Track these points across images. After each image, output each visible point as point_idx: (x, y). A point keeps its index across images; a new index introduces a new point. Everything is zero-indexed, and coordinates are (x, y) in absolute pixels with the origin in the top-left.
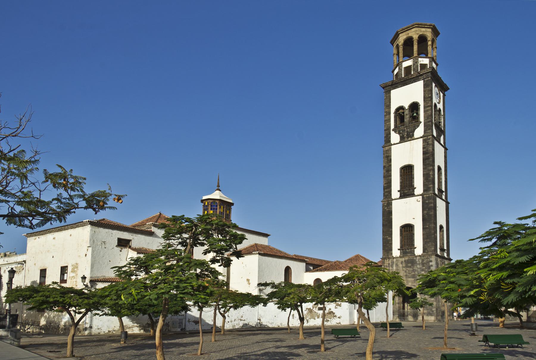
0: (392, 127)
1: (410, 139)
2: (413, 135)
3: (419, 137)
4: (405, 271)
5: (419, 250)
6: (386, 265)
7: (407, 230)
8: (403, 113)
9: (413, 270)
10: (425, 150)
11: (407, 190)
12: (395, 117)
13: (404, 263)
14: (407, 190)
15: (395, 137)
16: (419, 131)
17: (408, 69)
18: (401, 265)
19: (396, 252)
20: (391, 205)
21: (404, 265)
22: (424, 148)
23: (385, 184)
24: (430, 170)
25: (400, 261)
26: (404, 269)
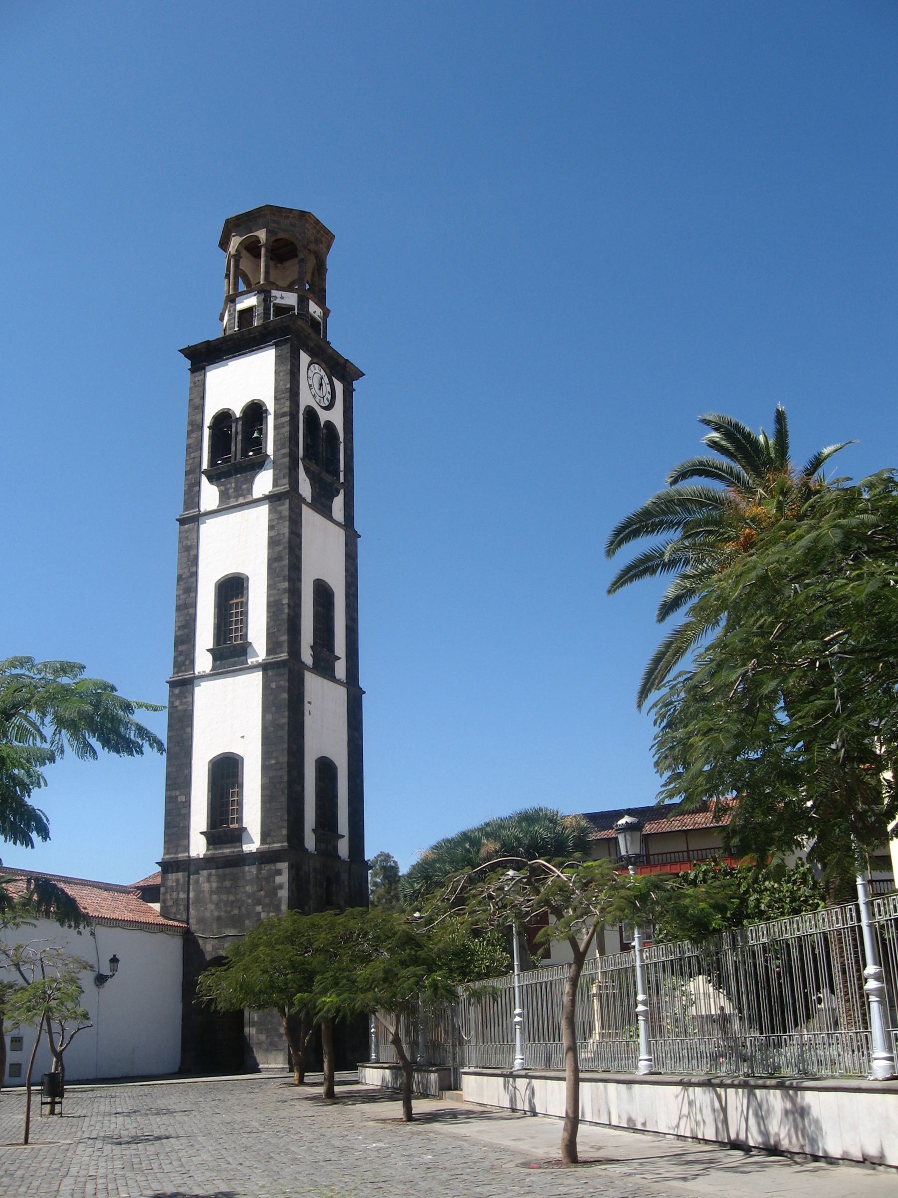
0: (205, 465)
1: (241, 500)
2: (250, 491)
4: (217, 905)
10: (273, 533)
12: (213, 438)
14: (230, 653)
15: (210, 495)
16: (264, 483)
17: (247, 314)
18: (206, 886)
21: (214, 885)
22: (271, 528)
26: (215, 897)
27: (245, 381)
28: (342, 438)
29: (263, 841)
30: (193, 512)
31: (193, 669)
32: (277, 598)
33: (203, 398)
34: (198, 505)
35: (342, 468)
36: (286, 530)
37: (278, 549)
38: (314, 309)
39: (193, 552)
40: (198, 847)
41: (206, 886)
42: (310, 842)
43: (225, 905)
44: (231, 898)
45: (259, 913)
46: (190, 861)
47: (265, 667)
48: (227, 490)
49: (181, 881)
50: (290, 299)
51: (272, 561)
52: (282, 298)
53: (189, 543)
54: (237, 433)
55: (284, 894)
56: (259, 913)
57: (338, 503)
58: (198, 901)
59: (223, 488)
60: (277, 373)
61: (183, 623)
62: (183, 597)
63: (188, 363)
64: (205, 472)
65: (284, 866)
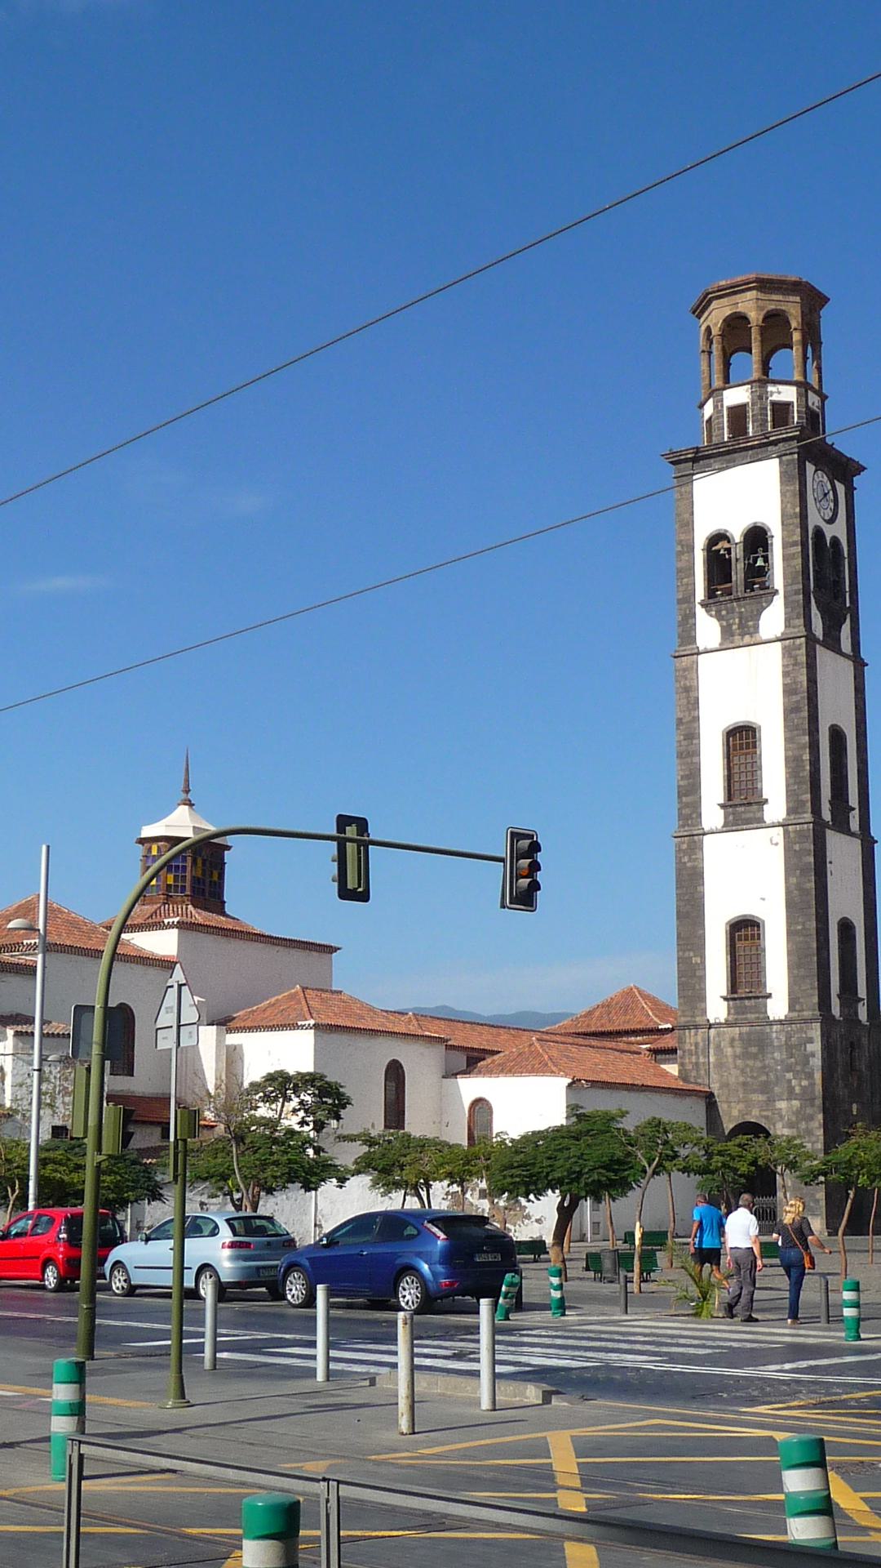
0: (700, 593)
1: (747, 639)
2: (756, 628)
3: (772, 637)
4: (743, 1071)
5: (778, 1007)
7: (744, 930)
8: (729, 550)
9: (764, 1067)
10: (788, 681)
11: (743, 804)
13: (737, 1043)
15: (707, 629)
16: (773, 619)
17: (738, 414)
18: (729, 1051)
19: (717, 1009)
21: (738, 1050)
22: (785, 674)
23: (682, 778)
26: (739, 1062)
27: (743, 497)
29: (791, 1008)
30: (689, 649)
32: (796, 753)
34: (693, 640)
36: (803, 678)
37: (795, 698)
38: (814, 400)
41: (729, 1051)
42: (836, 1010)
45: (789, 1081)
48: (730, 626)
51: (789, 711)
55: (817, 1062)
56: (789, 1081)
57: (846, 629)
58: (720, 1065)
60: (783, 494)
65: (816, 1031)
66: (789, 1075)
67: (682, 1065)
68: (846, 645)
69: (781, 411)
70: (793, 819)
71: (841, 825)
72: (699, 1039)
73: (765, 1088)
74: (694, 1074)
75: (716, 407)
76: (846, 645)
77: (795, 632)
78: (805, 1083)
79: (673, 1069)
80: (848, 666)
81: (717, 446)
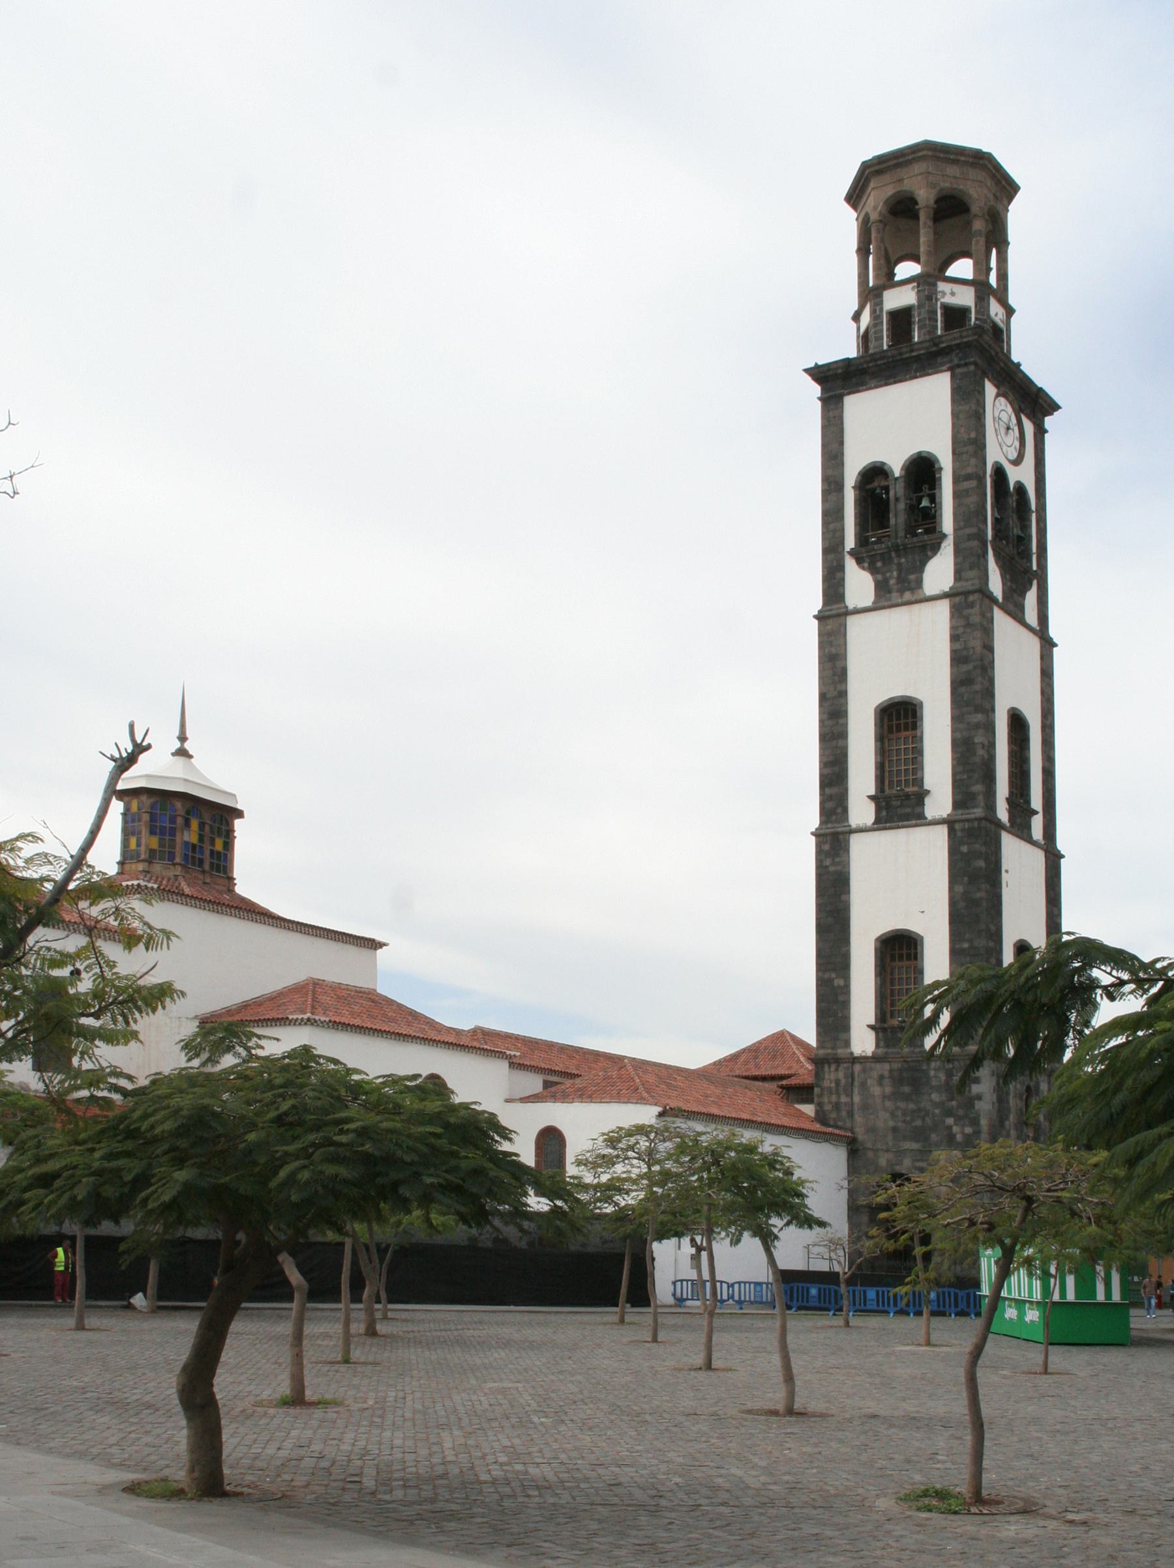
0: (850, 542)
1: (908, 596)
2: (919, 583)
4: (893, 1114)
6: (826, 1084)
7: (899, 949)
8: (887, 489)
10: (958, 646)
12: (861, 502)
13: (887, 1081)
15: (859, 585)
16: (940, 572)
17: (901, 318)
18: (876, 1091)
20: (847, 851)
21: (888, 1090)
22: (954, 638)
24: (977, 726)
25: (875, 1074)
26: (888, 1104)
28: (1033, 507)
30: (836, 608)
31: (847, 819)
33: (841, 443)
35: (1034, 549)
37: (965, 668)
39: (839, 664)
40: (863, 1041)
41: (876, 1091)
43: (904, 1114)
44: (912, 1106)
46: (854, 1060)
47: (950, 822)
48: (886, 581)
49: (843, 1081)
50: (965, 298)
52: (953, 294)
53: (833, 650)
54: (897, 499)
57: (1031, 598)
58: (865, 1107)
59: (879, 577)
61: (831, 758)
62: (830, 723)
63: (815, 390)
64: (852, 553)
66: (950, 1121)
67: (820, 1105)
68: (1031, 617)
69: (955, 315)
70: (961, 814)
71: (1021, 829)
72: (841, 1075)
73: (920, 1134)
74: (833, 1115)
75: (873, 312)
76: (1031, 617)
77: (968, 586)
78: (968, 1130)
79: (809, 1109)
80: (1034, 643)
81: (874, 358)
